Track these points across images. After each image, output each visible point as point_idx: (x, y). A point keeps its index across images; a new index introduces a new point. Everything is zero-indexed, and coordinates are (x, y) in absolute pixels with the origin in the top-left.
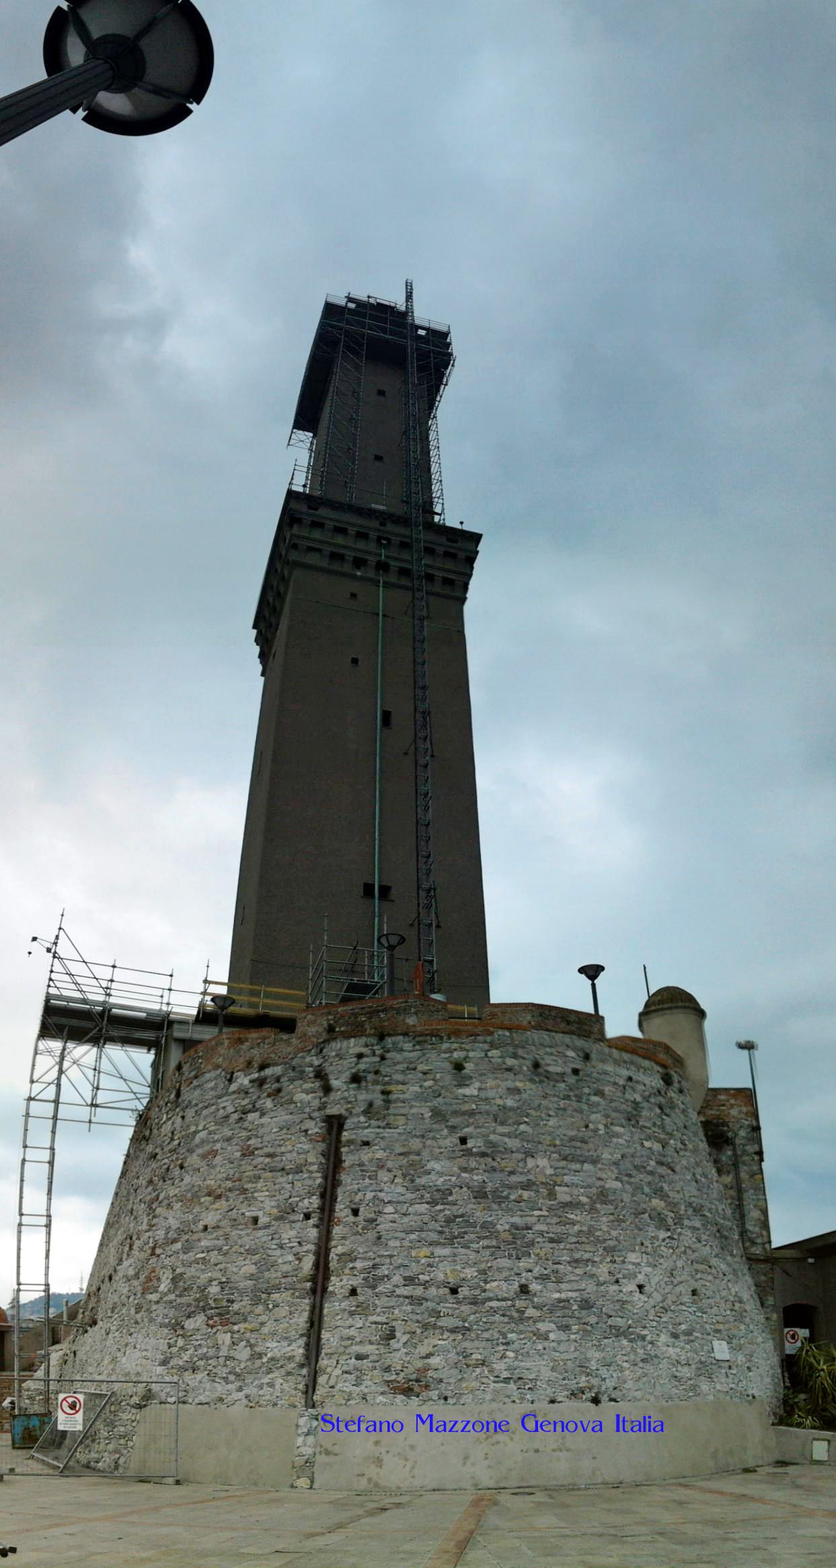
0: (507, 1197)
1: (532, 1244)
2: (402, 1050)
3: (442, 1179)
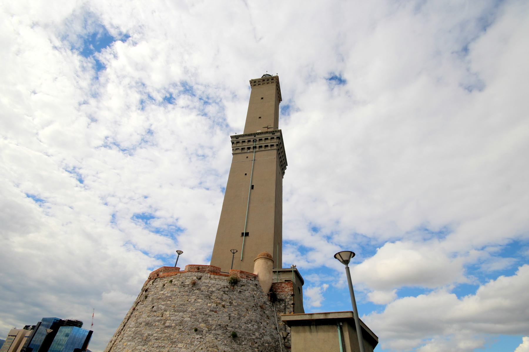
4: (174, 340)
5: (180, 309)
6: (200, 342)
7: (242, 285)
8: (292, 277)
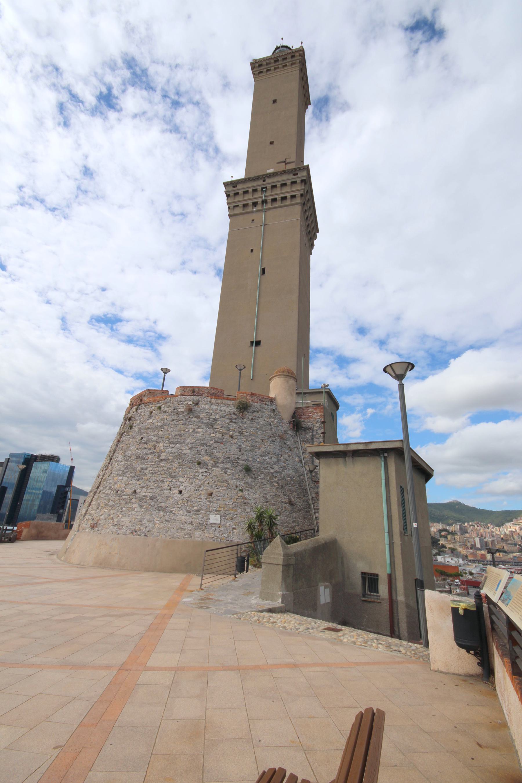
1: (145, 475)
4: (174, 474)
5: (177, 439)
6: (206, 476)
7: (254, 411)
8: (323, 400)
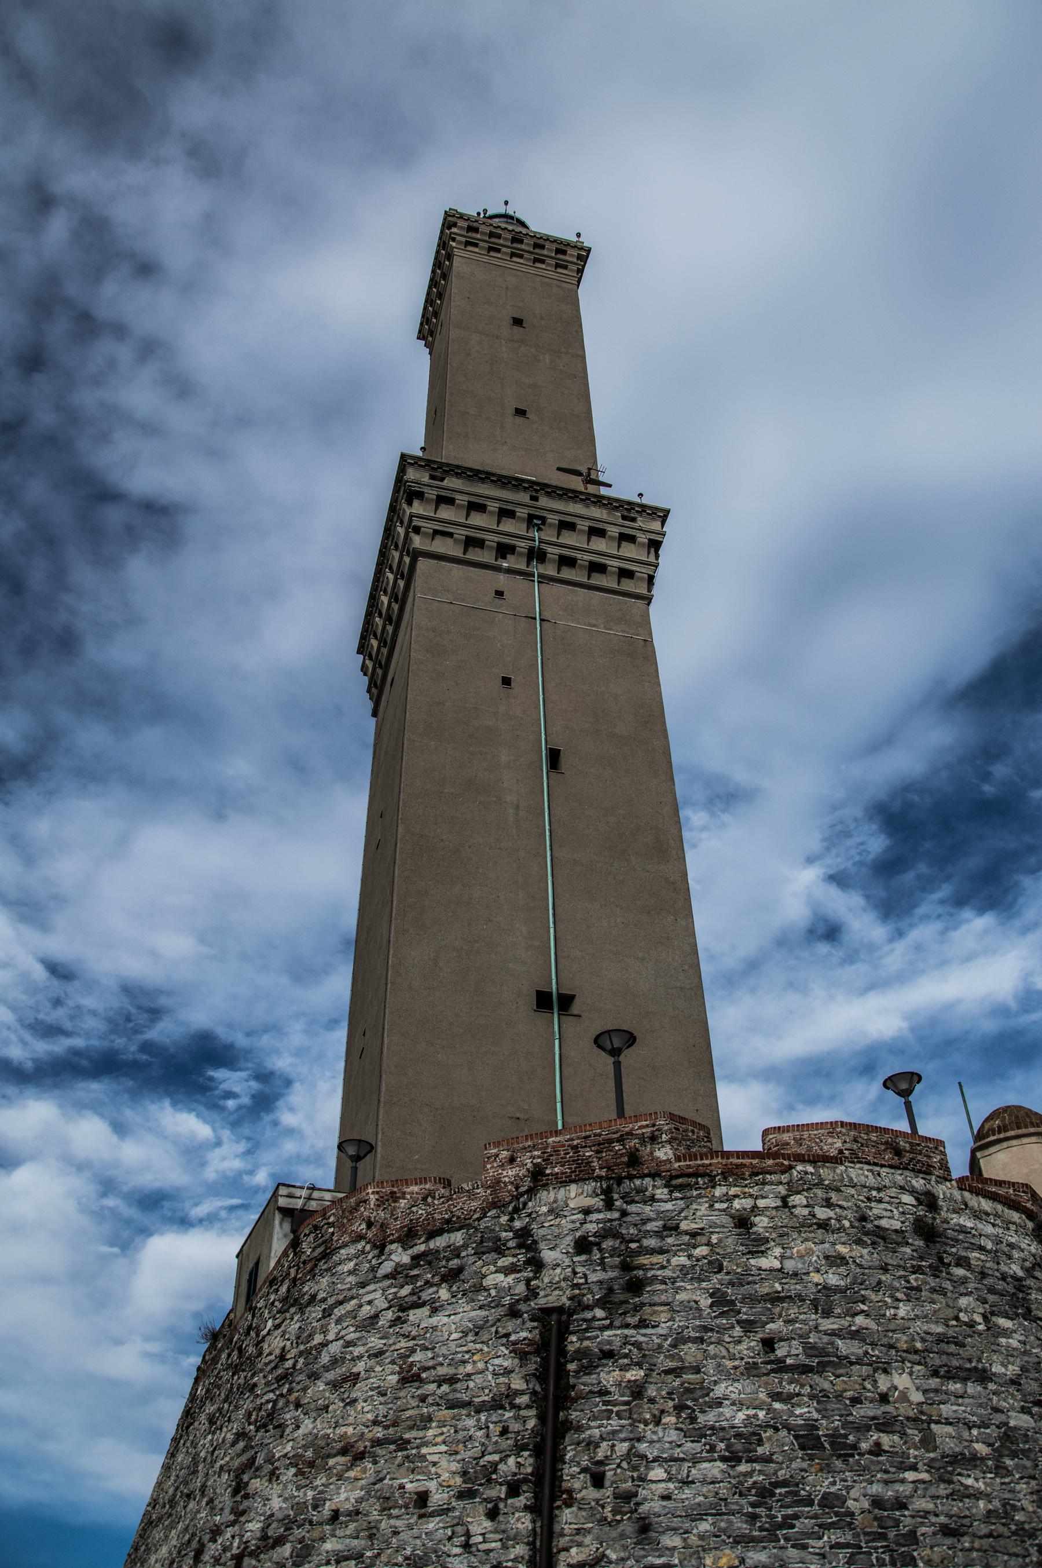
0: (854, 1447)
2: (653, 1199)
3: (741, 1416)
